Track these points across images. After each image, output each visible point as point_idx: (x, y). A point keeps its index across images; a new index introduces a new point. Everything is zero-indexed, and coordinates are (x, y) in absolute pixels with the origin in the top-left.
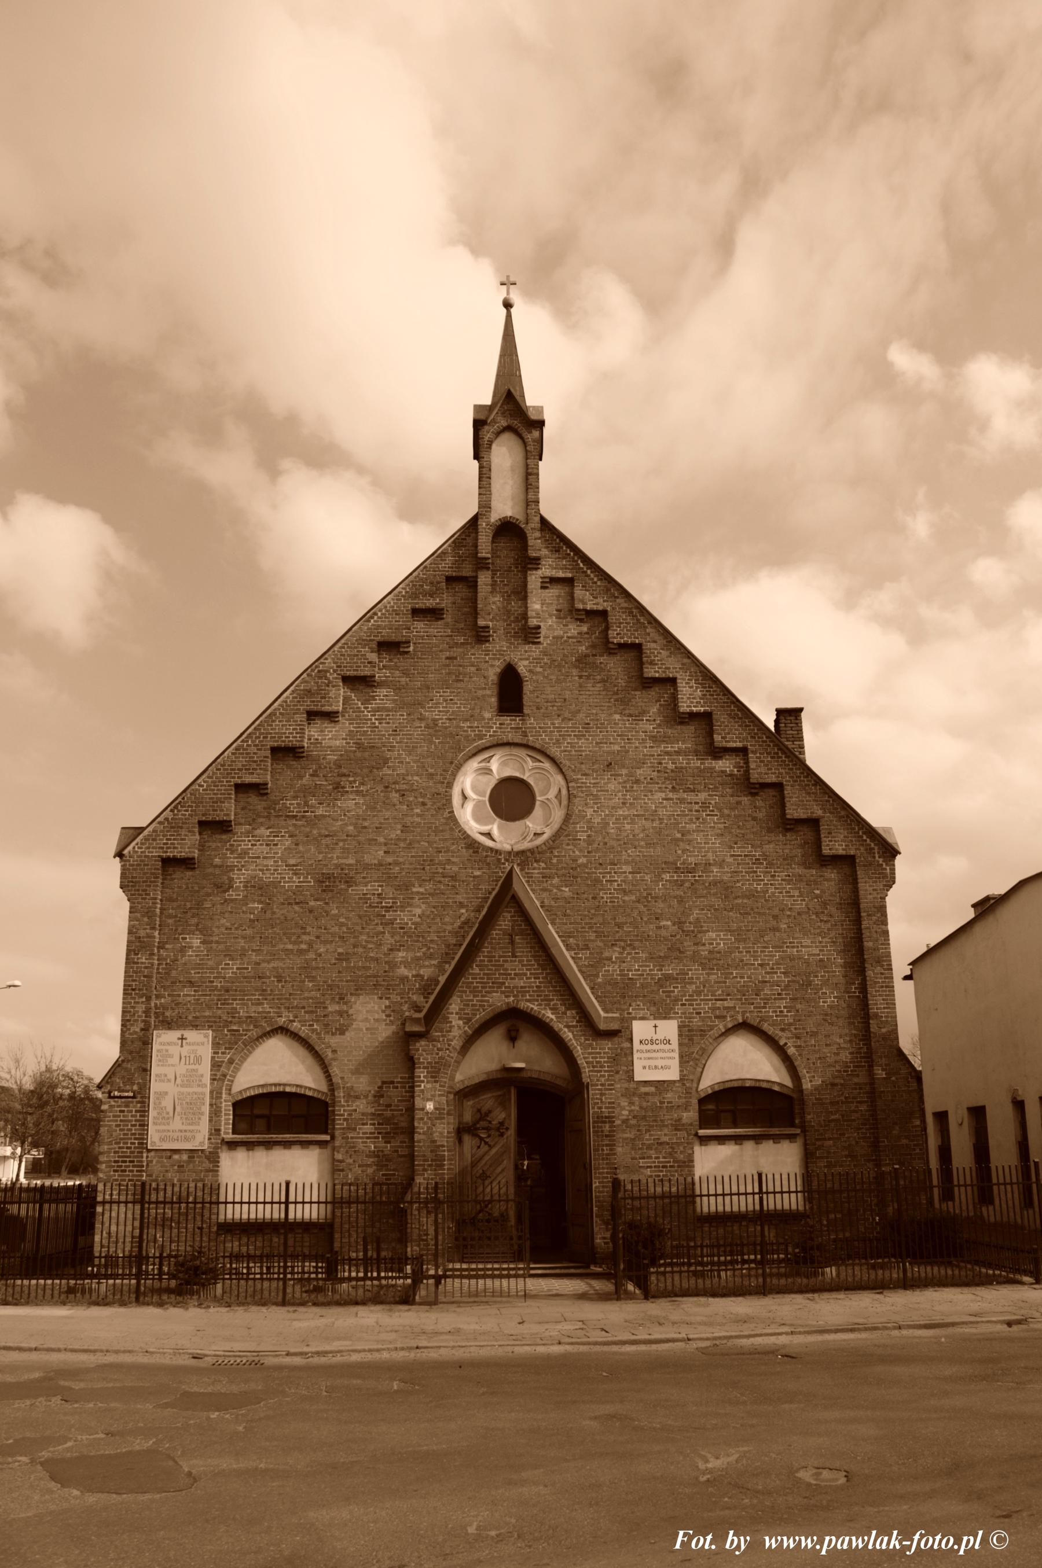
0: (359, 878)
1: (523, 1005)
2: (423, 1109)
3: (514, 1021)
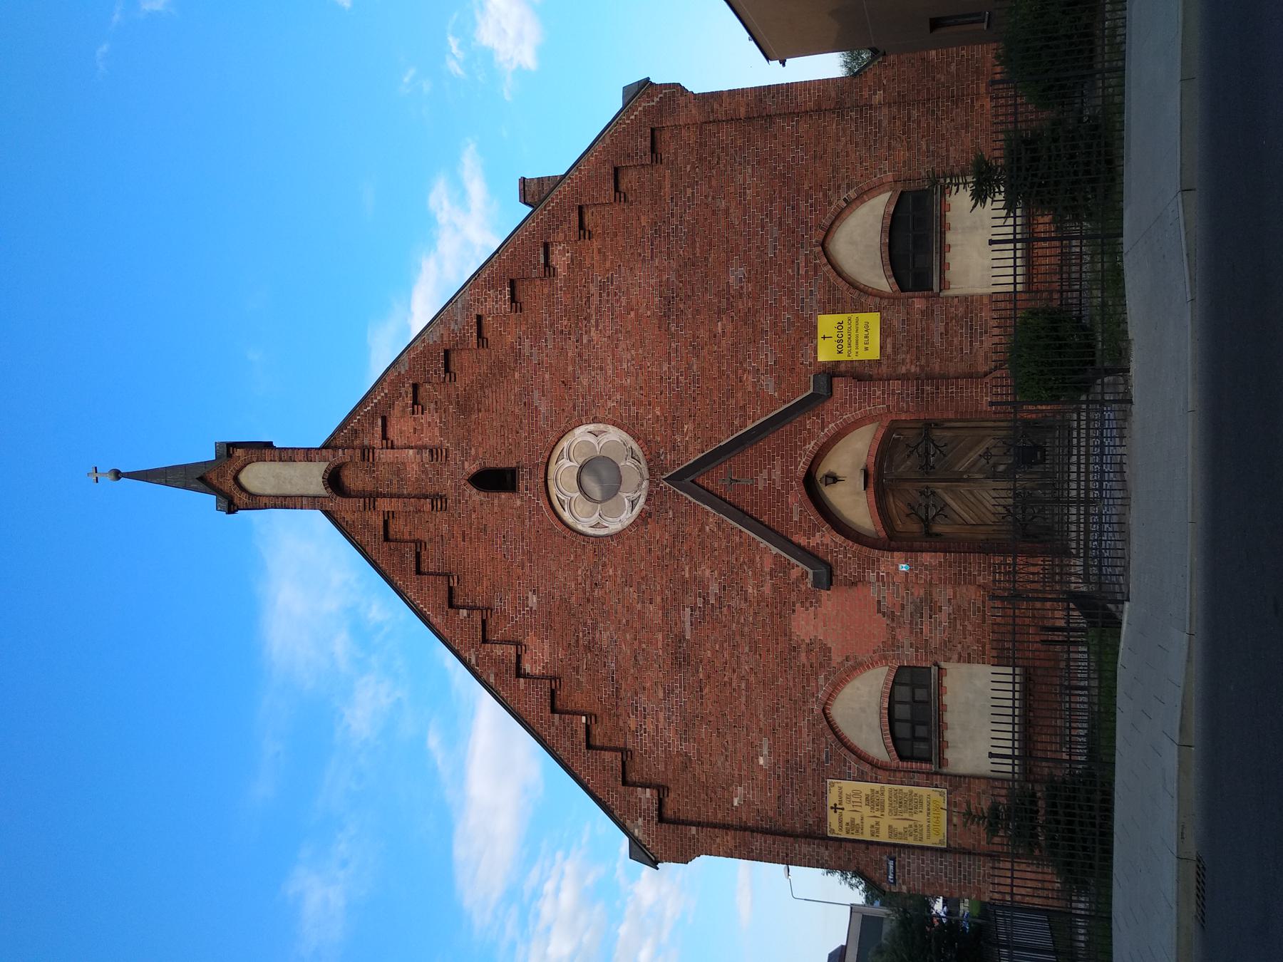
0: (676, 631)
1: (801, 469)
2: (906, 573)
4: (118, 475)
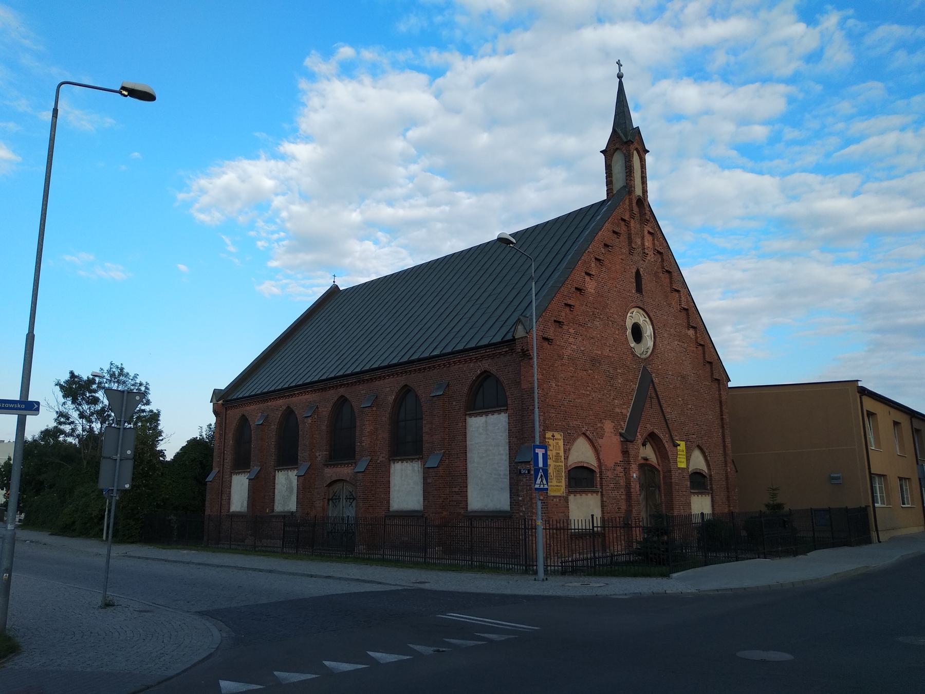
1: (656, 431)
4: (620, 76)
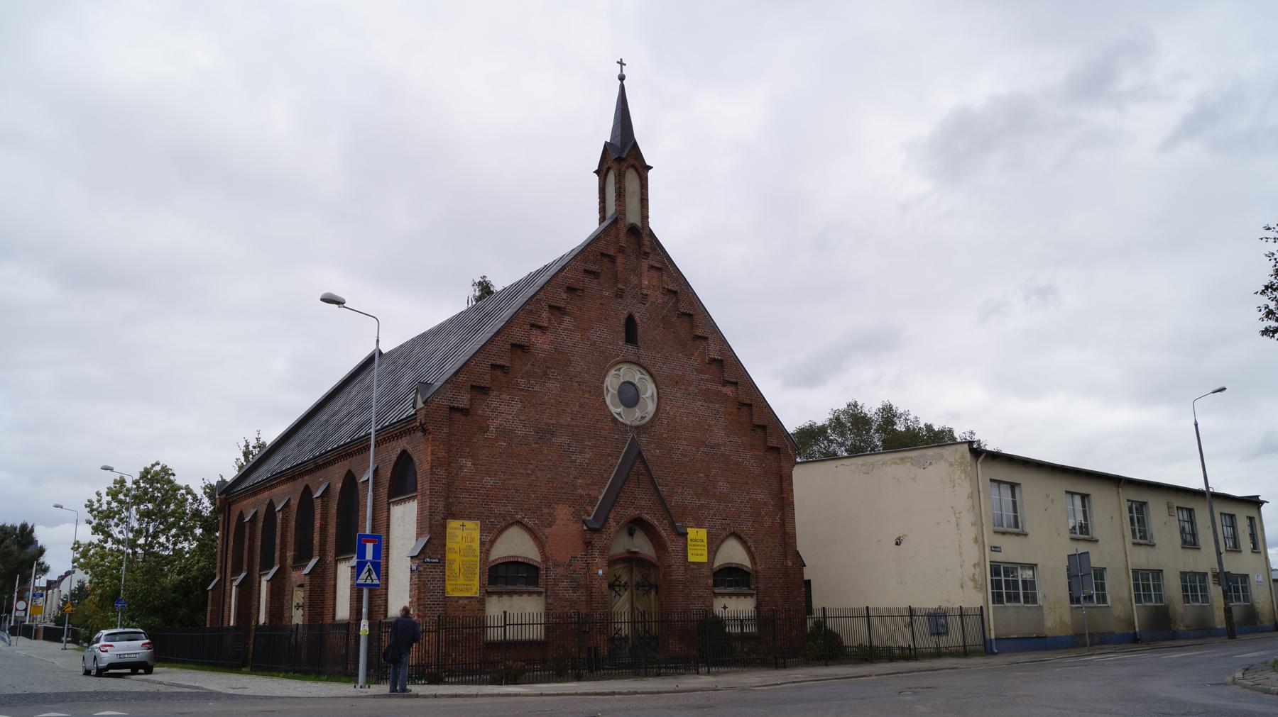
1: (646, 517)
3: (636, 525)
4: (622, 78)
